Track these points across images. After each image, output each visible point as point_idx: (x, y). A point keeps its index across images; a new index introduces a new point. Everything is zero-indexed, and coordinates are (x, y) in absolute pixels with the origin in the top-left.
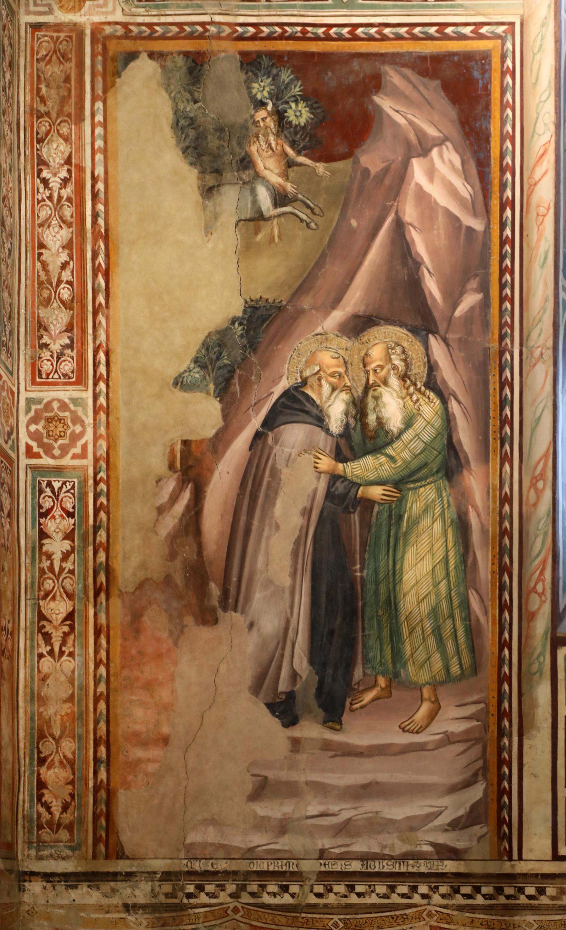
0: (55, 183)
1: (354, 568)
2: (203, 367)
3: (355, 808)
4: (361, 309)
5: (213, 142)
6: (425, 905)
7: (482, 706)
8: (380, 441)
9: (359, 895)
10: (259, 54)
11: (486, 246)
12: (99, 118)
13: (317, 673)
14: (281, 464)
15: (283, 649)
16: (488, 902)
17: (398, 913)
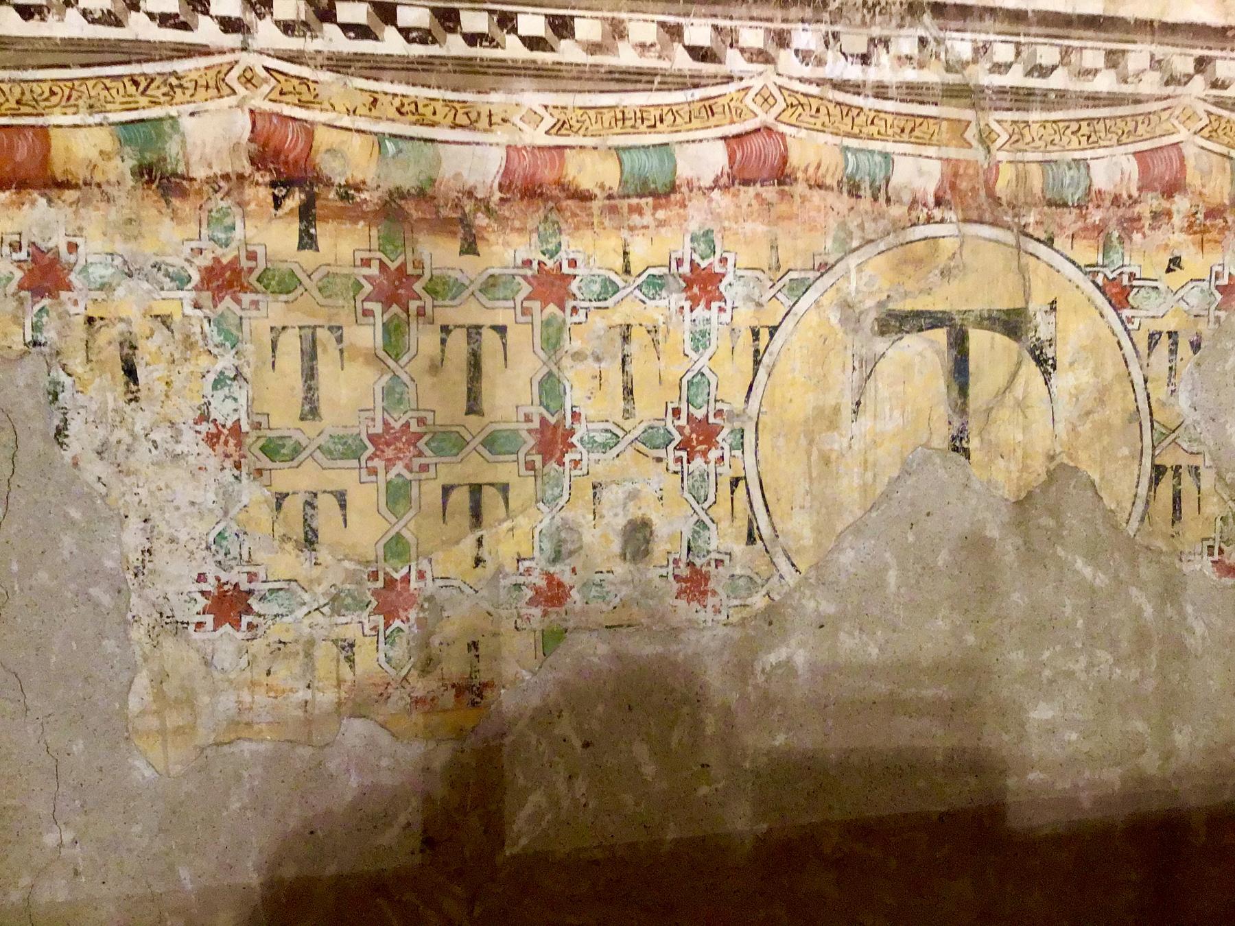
6: (233, 50)
16: (418, 50)
17: (150, 68)
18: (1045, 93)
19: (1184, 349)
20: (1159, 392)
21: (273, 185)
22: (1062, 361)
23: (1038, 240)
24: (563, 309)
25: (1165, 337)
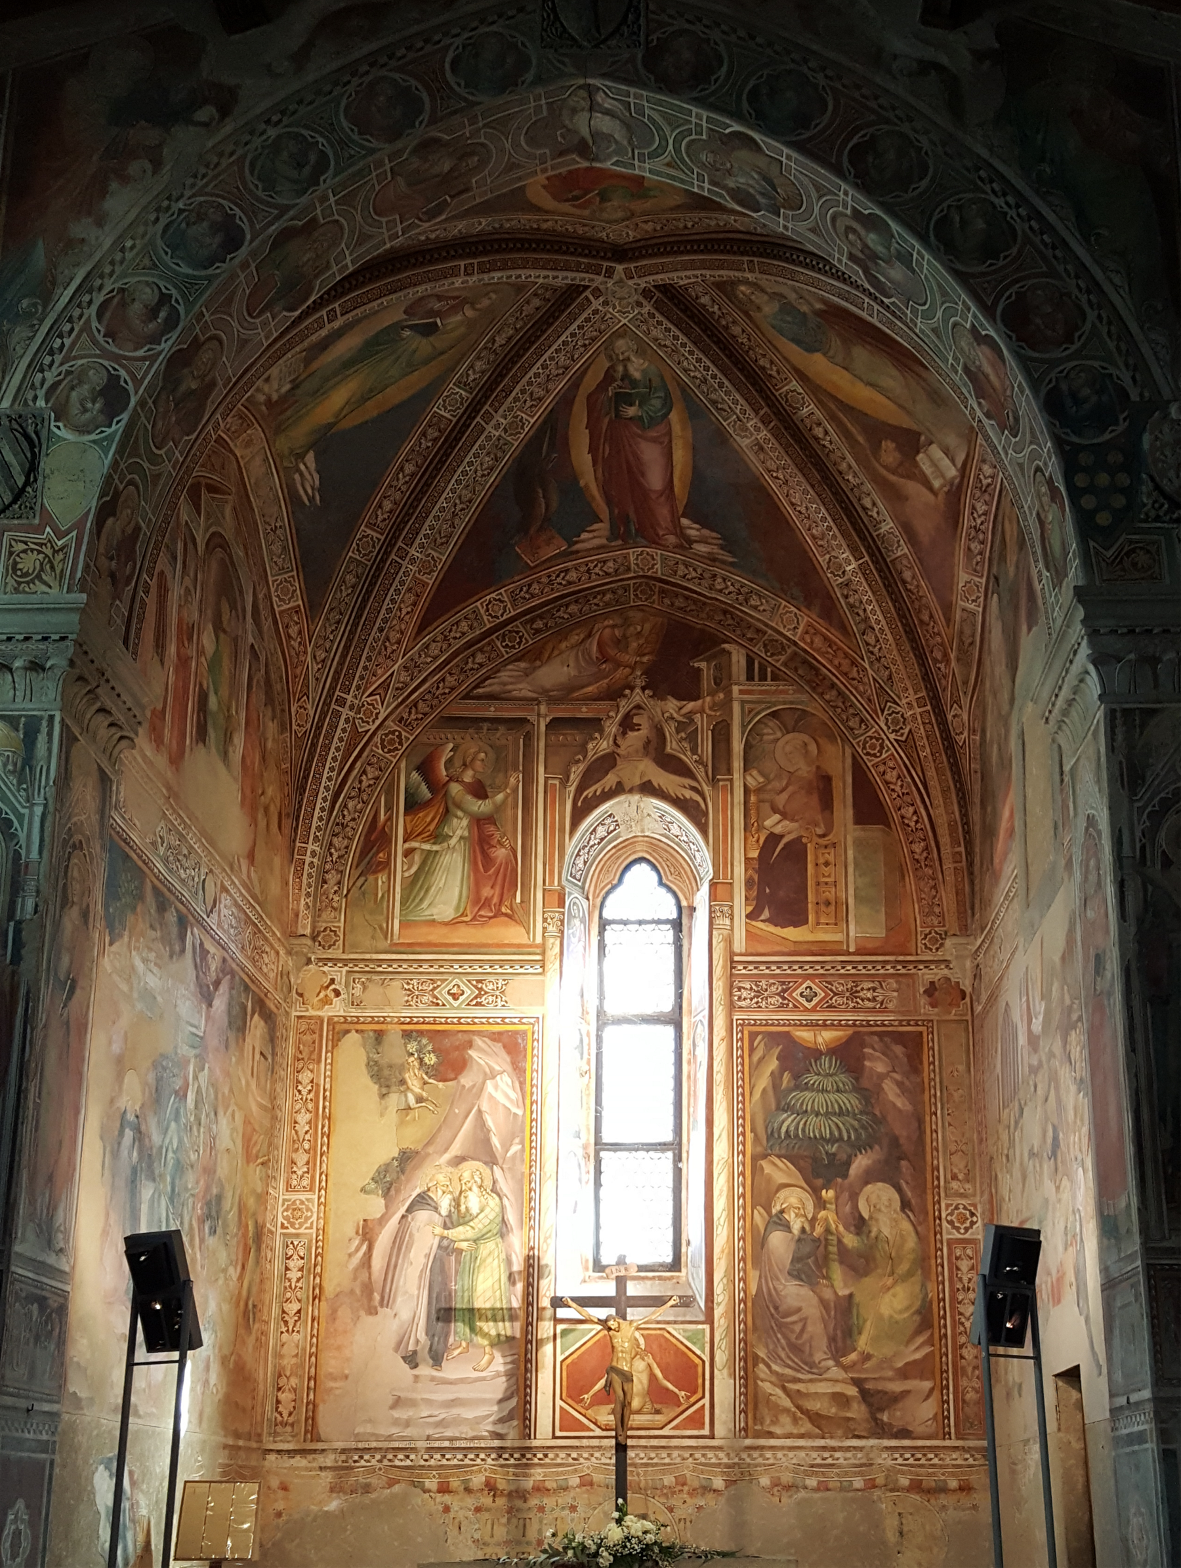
0: (304, 1092)
2: (376, 1182)
4: (459, 1153)
5: (386, 1072)
8: (467, 1219)
10: (412, 1031)
11: (523, 1122)
12: (329, 1061)
14: (415, 1232)
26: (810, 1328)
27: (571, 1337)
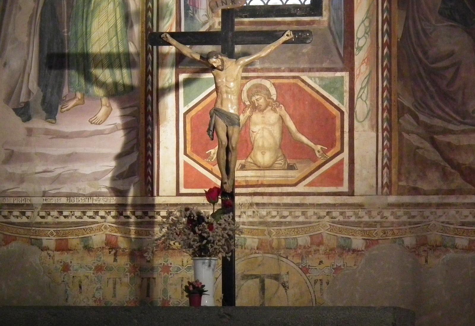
1: (63, 31)
3: (63, 168)
6: (103, 222)
7: (136, 108)
9: (65, 217)
13: (42, 91)
15: (23, 77)
17: (87, 227)
18: (285, 222)
19: (325, 284)
20: (318, 294)
21: (109, 249)
22: (290, 287)
23: (284, 257)
24: (168, 274)
25: (319, 281)
26: (463, 74)
27: (195, 86)
